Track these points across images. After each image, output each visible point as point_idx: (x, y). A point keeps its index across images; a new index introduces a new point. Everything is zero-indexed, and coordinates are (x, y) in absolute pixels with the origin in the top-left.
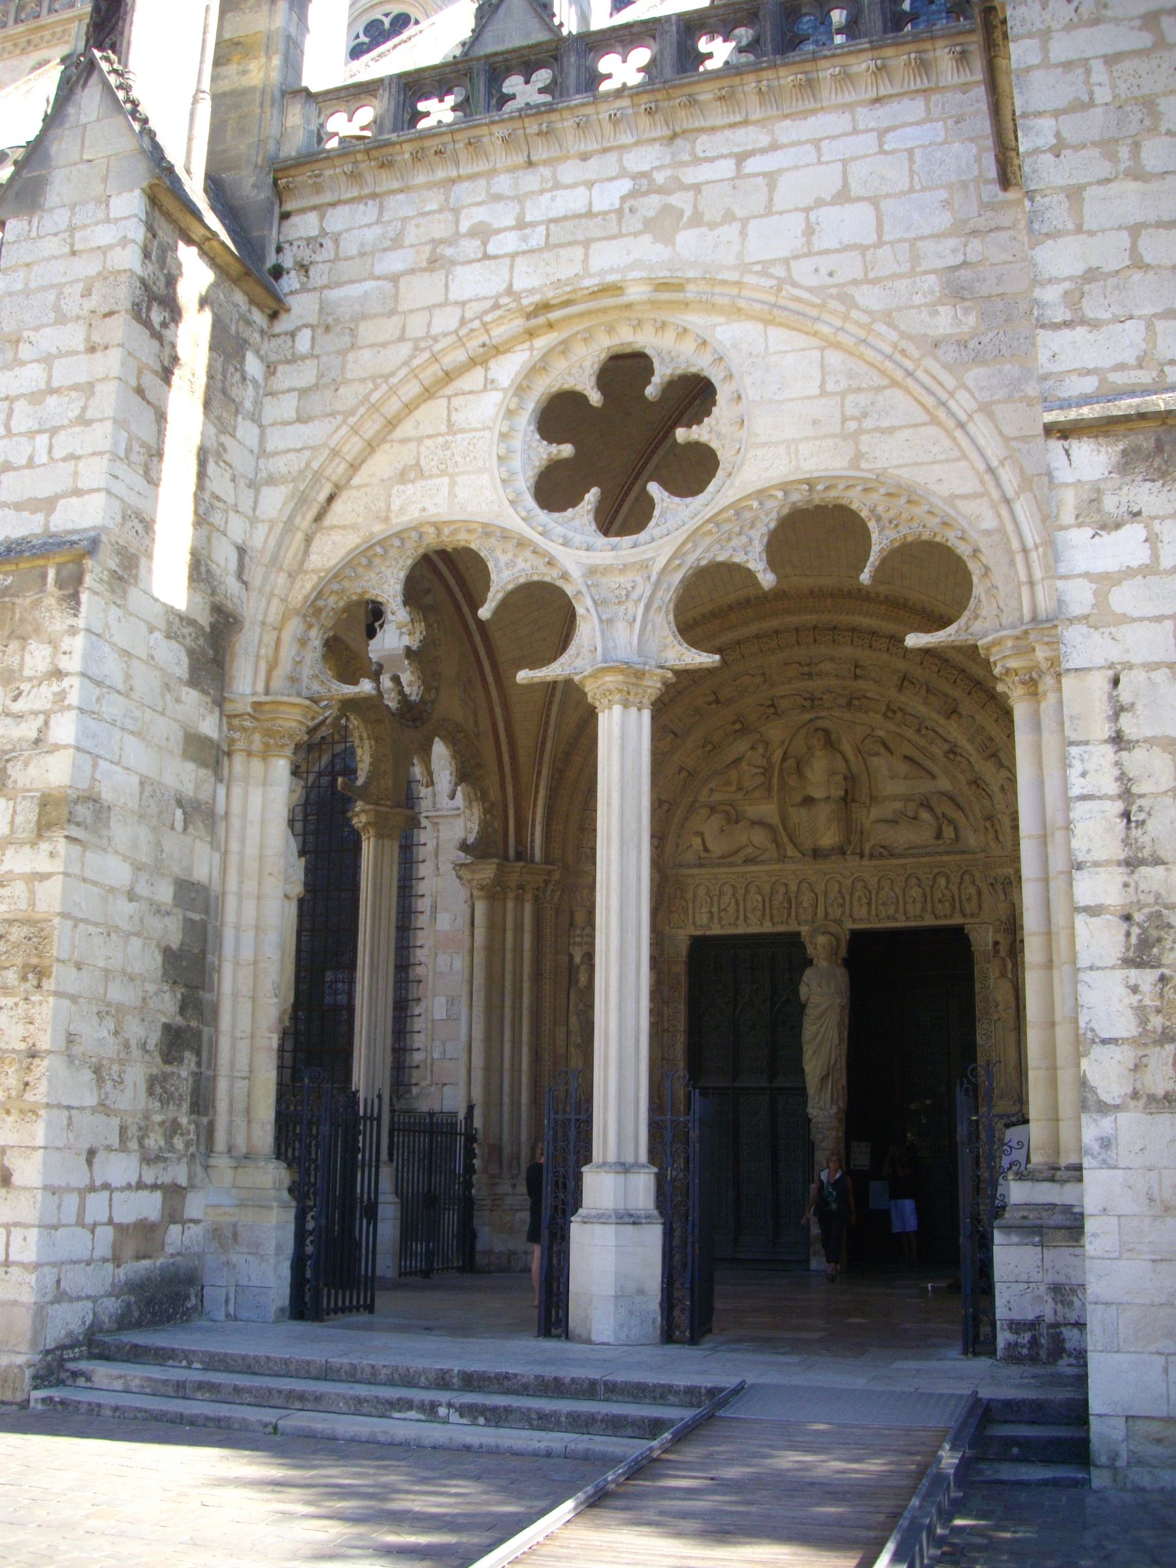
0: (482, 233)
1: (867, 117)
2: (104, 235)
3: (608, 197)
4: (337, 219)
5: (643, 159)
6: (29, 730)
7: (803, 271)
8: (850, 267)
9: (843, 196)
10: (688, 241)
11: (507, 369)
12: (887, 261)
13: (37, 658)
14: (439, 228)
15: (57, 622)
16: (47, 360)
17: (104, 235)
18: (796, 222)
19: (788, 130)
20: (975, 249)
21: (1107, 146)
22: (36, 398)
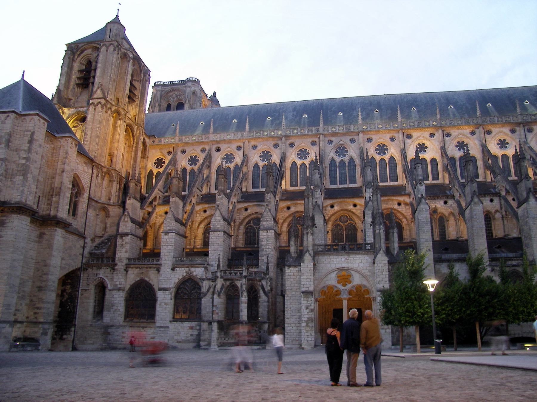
0: (333, 261)
1: (363, 256)
2: (310, 266)
3: (343, 259)
4: (320, 257)
5: (346, 257)
6: (310, 304)
7: (358, 268)
8: (362, 268)
9: (361, 263)
10: (349, 264)
11: (335, 273)
12: (364, 268)
13: (310, 299)
14: (330, 260)
15: (311, 297)
16: (307, 276)
17: (310, 266)
18: (358, 264)
19: (357, 256)
20: (371, 268)
21: (381, 272)
22: (306, 279)
